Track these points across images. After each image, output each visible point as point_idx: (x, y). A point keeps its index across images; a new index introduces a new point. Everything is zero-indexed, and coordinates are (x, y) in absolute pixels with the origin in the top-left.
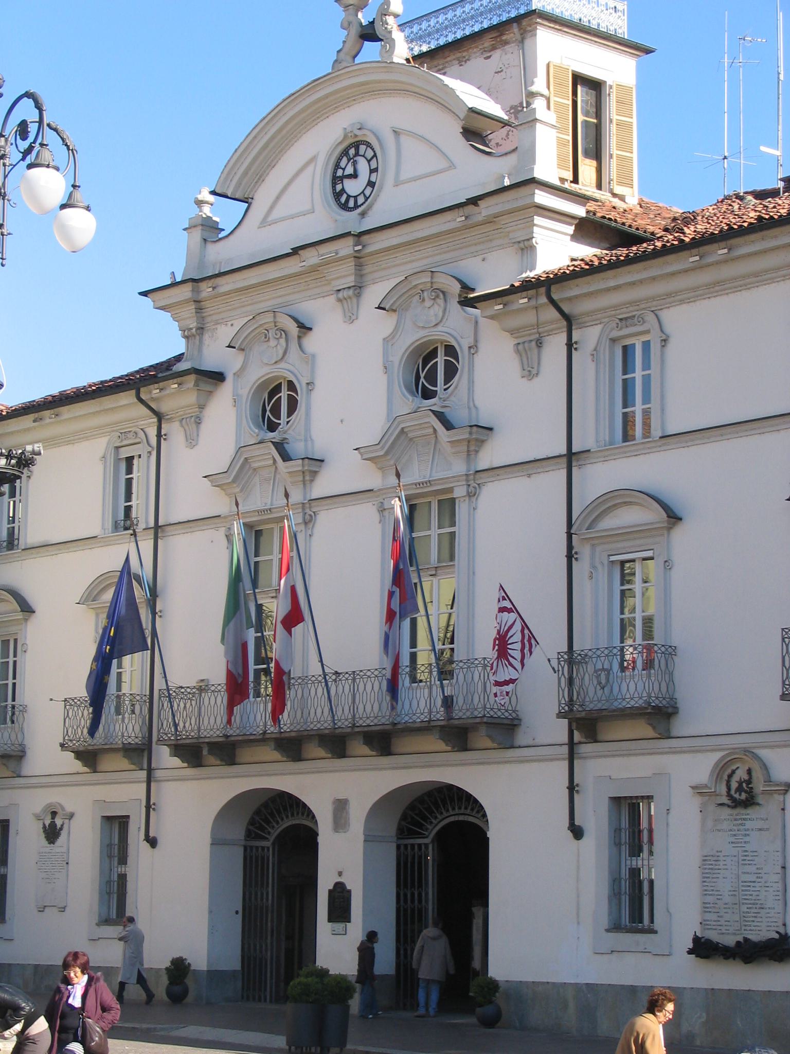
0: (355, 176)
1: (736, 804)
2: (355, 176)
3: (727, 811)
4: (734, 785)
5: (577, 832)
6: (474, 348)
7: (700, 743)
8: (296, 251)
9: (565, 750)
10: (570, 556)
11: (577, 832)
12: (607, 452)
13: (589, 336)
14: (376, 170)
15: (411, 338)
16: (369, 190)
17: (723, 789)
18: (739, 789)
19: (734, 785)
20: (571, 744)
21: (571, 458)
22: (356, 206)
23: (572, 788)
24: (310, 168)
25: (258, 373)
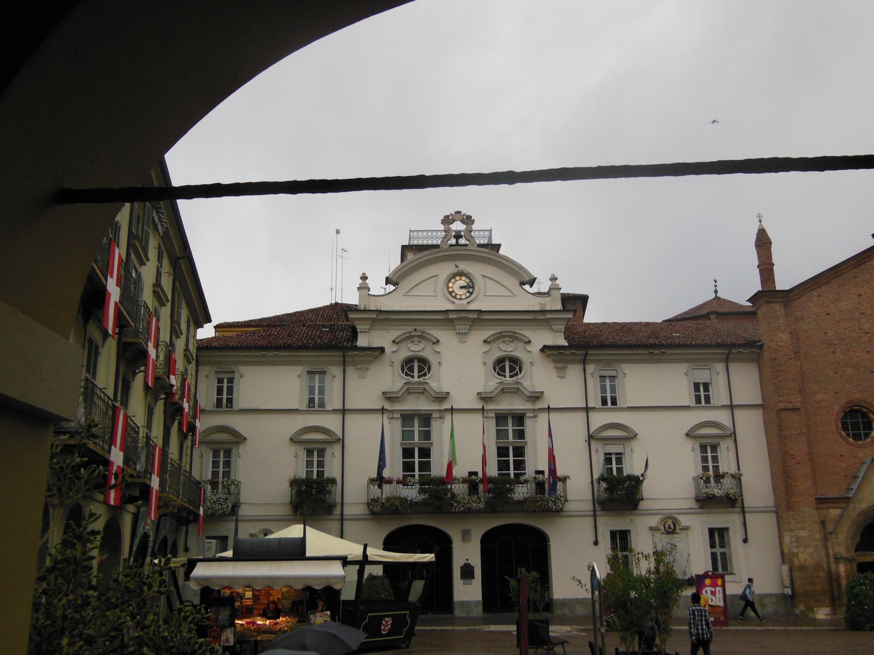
0: (462, 287)
1: (668, 533)
2: (462, 287)
3: (664, 535)
4: (667, 526)
5: (596, 543)
6: (532, 363)
7: (651, 513)
8: (447, 311)
9: (592, 513)
10: (589, 444)
11: (596, 543)
12: (599, 410)
13: (590, 368)
14: (473, 287)
15: (497, 354)
16: (468, 295)
17: (662, 528)
18: (669, 527)
19: (667, 526)
20: (594, 511)
21: (587, 409)
22: (461, 299)
23: (596, 527)
24: (433, 280)
25: (405, 353)
